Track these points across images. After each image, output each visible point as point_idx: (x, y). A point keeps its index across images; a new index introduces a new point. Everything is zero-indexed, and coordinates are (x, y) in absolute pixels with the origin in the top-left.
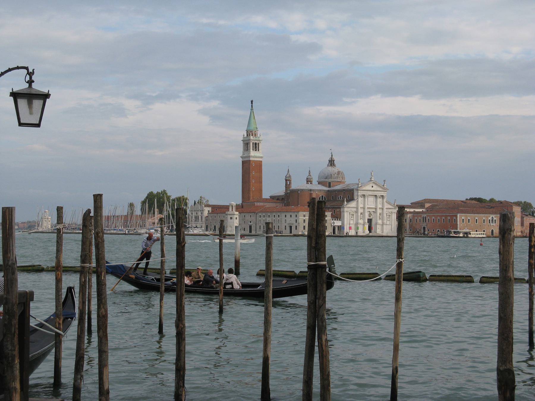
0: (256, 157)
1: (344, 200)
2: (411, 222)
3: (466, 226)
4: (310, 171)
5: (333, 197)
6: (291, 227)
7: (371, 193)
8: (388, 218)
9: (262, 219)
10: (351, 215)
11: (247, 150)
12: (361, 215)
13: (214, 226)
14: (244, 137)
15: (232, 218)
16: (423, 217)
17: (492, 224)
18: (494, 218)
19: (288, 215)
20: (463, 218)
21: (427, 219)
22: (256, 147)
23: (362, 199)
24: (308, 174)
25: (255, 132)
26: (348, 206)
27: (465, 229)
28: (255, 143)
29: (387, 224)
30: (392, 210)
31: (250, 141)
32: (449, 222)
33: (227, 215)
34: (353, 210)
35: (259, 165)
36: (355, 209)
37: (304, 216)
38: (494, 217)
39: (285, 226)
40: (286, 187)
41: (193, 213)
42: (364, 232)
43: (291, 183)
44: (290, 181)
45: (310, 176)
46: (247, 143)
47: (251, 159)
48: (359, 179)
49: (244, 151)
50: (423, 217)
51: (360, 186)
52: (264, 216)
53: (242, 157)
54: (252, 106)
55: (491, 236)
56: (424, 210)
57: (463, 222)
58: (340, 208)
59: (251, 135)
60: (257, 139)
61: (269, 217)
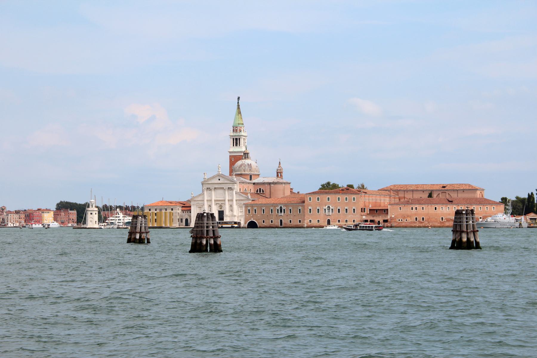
0: (235, 152)
3: (252, 217)
4: (280, 163)
7: (217, 186)
12: (210, 208)
17: (279, 214)
18: (283, 207)
20: (249, 208)
23: (209, 192)
25: (236, 128)
28: (236, 138)
30: (245, 201)
38: (283, 207)
54: (238, 103)
55: (280, 226)
60: (238, 134)
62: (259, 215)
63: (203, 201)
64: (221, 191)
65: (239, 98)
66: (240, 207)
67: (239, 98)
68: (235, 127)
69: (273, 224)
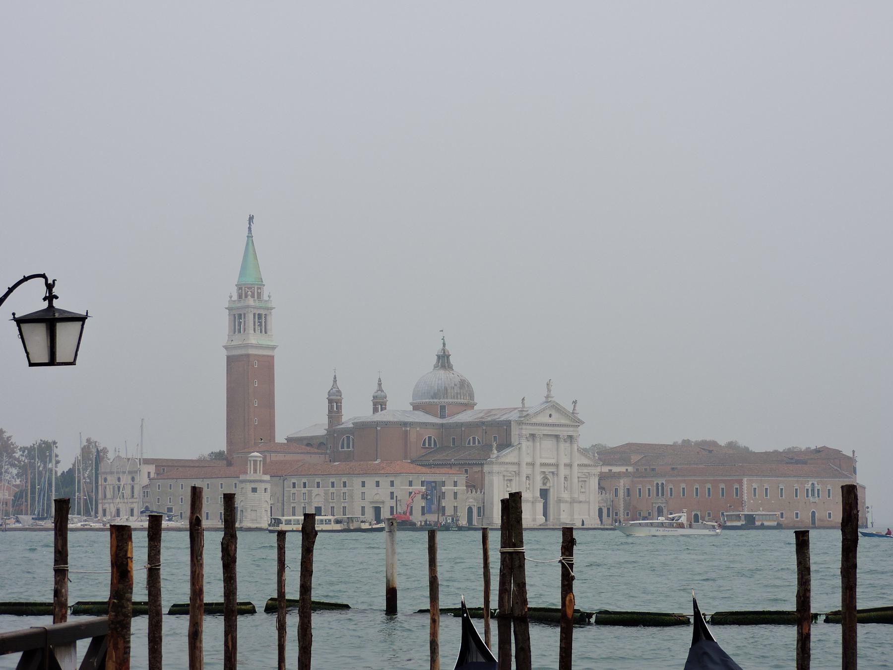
1: (491, 446)
2: (628, 495)
4: (380, 380)
5: (454, 439)
6: (377, 510)
8: (582, 487)
9: (301, 490)
10: (507, 480)
11: (239, 331)
13: (168, 508)
14: (231, 301)
15: (256, 488)
16: (657, 484)
17: (811, 499)
18: (816, 485)
19: (370, 482)
20: (755, 485)
21: (667, 489)
22: (261, 322)
23: (530, 443)
24: (376, 387)
25: (258, 288)
26: (500, 460)
27: (760, 510)
28: (259, 314)
29: (580, 502)
30: (589, 468)
31: (247, 310)
32: (723, 495)
33: (242, 482)
34: (511, 470)
35: (268, 364)
36: (515, 468)
37: (411, 484)
38: (816, 483)
39: (363, 508)
40: (330, 417)
41: (109, 478)
42: (534, 520)
43: (341, 406)
44: (339, 402)
45: (382, 391)
46: (240, 315)
47: (252, 351)
48: (523, 399)
49: (232, 333)
50: (657, 484)
51: (525, 414)
52: (305, 484)
53: (226, 348)
54: (250, 228)
56: (630, 469)
57: (755, 495)
58: (482, 464)
59: (249, 297)
61: (318, 487)
62: (773, 502)
63: (519, 464)
64: (548, 444)
65: (251, 219)
66: (582, 481)
67: (251, 219)
68: (256, 287)
69: (798, 522)
